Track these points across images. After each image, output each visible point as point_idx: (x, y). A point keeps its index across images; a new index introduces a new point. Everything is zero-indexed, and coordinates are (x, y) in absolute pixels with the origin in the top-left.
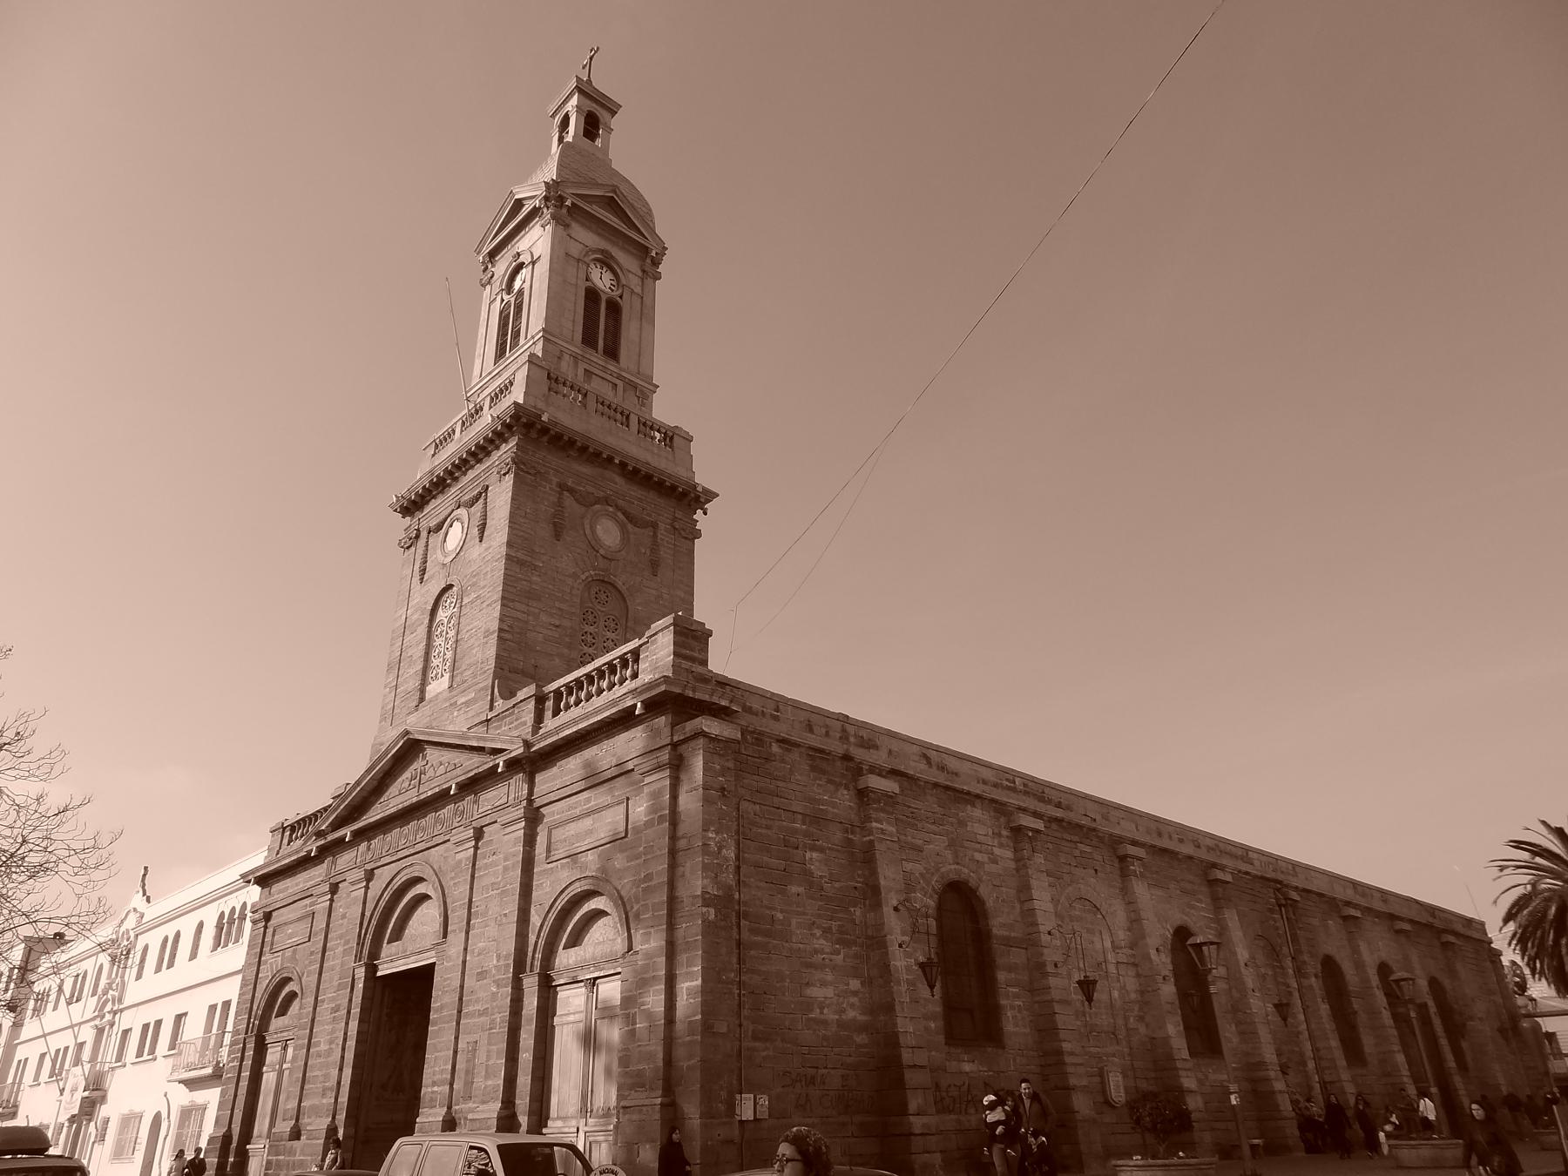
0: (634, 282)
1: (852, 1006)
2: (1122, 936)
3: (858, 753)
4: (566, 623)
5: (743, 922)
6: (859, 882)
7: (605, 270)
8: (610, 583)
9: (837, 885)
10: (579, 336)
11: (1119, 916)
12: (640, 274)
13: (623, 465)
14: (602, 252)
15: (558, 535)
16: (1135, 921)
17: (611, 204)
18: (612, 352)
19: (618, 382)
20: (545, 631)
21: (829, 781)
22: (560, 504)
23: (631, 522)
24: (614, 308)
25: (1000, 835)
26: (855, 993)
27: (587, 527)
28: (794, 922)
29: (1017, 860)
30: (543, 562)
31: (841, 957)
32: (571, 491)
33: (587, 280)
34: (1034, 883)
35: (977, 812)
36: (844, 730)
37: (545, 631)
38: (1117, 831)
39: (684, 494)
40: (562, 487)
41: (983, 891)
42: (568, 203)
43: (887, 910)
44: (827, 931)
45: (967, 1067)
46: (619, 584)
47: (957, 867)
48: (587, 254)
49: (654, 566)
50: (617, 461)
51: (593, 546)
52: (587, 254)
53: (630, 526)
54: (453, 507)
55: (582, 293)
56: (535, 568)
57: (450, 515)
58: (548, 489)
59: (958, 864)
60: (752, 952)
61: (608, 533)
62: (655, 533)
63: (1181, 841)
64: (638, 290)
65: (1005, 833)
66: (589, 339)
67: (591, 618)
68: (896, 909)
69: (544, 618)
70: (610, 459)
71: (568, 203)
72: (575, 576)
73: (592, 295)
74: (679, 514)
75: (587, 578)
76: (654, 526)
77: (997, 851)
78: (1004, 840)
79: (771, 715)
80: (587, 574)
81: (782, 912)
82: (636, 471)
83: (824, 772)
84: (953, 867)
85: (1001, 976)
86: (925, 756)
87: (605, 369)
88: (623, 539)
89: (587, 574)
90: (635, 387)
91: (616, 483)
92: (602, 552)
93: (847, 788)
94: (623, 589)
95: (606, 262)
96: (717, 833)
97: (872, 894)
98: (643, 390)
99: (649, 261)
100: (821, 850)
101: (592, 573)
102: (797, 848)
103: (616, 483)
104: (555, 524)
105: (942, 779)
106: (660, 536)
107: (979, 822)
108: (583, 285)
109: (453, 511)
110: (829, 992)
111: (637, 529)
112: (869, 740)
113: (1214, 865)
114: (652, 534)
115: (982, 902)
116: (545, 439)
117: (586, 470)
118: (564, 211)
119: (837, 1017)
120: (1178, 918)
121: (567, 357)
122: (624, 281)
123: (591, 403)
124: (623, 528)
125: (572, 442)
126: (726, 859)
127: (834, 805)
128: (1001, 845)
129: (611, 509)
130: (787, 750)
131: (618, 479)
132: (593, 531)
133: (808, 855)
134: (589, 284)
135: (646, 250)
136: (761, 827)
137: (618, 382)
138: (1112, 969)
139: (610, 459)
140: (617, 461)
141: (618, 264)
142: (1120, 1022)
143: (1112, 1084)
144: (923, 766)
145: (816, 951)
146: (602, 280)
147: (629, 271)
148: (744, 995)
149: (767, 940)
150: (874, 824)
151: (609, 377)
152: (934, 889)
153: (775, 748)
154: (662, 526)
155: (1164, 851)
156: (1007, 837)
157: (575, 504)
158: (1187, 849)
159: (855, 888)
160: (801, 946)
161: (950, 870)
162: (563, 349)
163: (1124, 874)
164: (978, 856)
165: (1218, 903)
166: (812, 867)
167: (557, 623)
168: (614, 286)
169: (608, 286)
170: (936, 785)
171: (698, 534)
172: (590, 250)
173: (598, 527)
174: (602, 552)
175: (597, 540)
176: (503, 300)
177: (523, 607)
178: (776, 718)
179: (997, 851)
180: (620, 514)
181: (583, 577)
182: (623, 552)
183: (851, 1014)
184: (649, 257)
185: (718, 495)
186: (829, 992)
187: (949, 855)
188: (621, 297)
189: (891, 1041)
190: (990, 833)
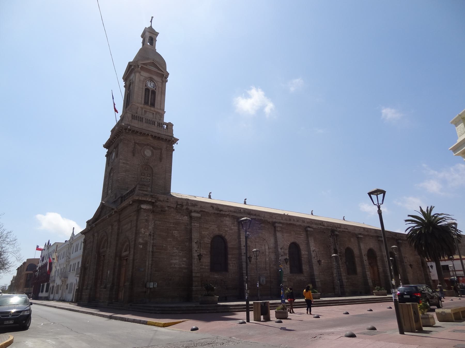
0: (160, 84)
1: (183, 264)
2: (272, 245)
3: (190, 208)
5: (154, 247)
6: (188, 237)
7: (151, 82)
9: (182, 238)
10: (143, 102)
11: (272, 240)
12: (161, 81)
13: (152, 136)
14: (150, 78)
15: (134, 155)
16: (276, 242)
17: (153, 64)
18: (153, 105)
19: (154, 112)
24: (154, 93)
26: (185, 261)
27: (142, 152)
28: (168, 247)
30: (130, 162)
31: (181, 253)
32: (138, 144)
33: (146, 86)
35: (228, 219)
36: (187, 202)
38: (274, 220)
39: (170, 141)
41: (226, 237)
42: (140, 67)
44: (177, 249)
45: (216, 277)
47: (219, 232)
48: (146, 79)
49: (161, 159)
50: (150, 135)
52: (146, 79)
53: (154, 151)
55: (144, 90)
56: (128, 164)
58: (131, 144)
59: (219, 231)
60: (156, 254)
61: (148, 153)
62: (161, 151)
63: (298, 221)
64: (161, 86)
66: (146, 103)
67: (143, 174)
70: (148, 135)
71: (140, 67)
73: (147, 90)
74: (168, 146)
75: (142, 165)
76: (161, 149)
77: (232, 227)
79: (166, 201)
80: (142, 164)
81: (165, 245)
82: (155, 137)
83: (180, 213)
84: (218, 232)
85: (229, 256)
86: (212, 206)
87: (150, 110)
88: (152, 154)
90: (159, 113)
91: (150, 140)
92: (146, 158)
93: (187, 216)
95: (151, 80)
96: (144, 229)
97: (190, 240)
98: (161, 114)
99: (164, 78)
100: (178, 230)
101: (143, 163)
102: (171, 230)
103: (150, 140)
104: (133, 153)
105: (216, 212)
106: (162, 152)
107: (228, 221)
108: (144, 88)
110: (177, 261)
112: (195, 204)
113: (309, 227)
114: (160, 152)
116: (130, 132)
118: (139, 68)
119: (179, 266)
120: (292, 240)
121: (139, 108)
122: (156, 84)
123: (144, 120)
125: (137, 132)
126: (146, 235)
127: (183, 220)
128: (234, 226)
129: (149, 147)
130: (170, 208)
132: (144, 153)
133: (174, 232)
134: (146, 87)
135: (163, 75)
136: (161, 226)
137: (154, 112)
138: (267, 253)
139: (148, 135)
140: (150, 135)
141: (155, 80)
143: (261, 280)
144: (211, 209)
145: (174, 253)
146: (150, 85)
147: (158, 81)
148: (153, 262)
149: (161, 251)
150: (193, 224)
151: (151, 112)
152: (211, 237)
153: (166, 208)
154: (163, 149)
155: (291, 224)
156: (236, 224)
158: (298, 223)
159: (187, 238)
160: (170, 252)
161: (217, 232)
162: (139, 106)
163: (275, 231)
164: (226, 229)
165: (308, 235)
166: (175, 234)
167: (134, 177)
168: (154, 86)
169: (152, 86)
170: (214, 213)
171: (174, 150)
172: (147, 78)
173: (145, 152)
174: (146, 158)
176: (127, 92)
177: (124, 174)
178: (168, 202)
180: (151, 148)
181: (141, 165)
182: (152, 157)
183: (183, 266)
184: (164, 76)
185: (179, 140)
186: (177, 261)
187: (217, 229)
188: (156, 89)
189: (191, 272)
190: (231, 223)
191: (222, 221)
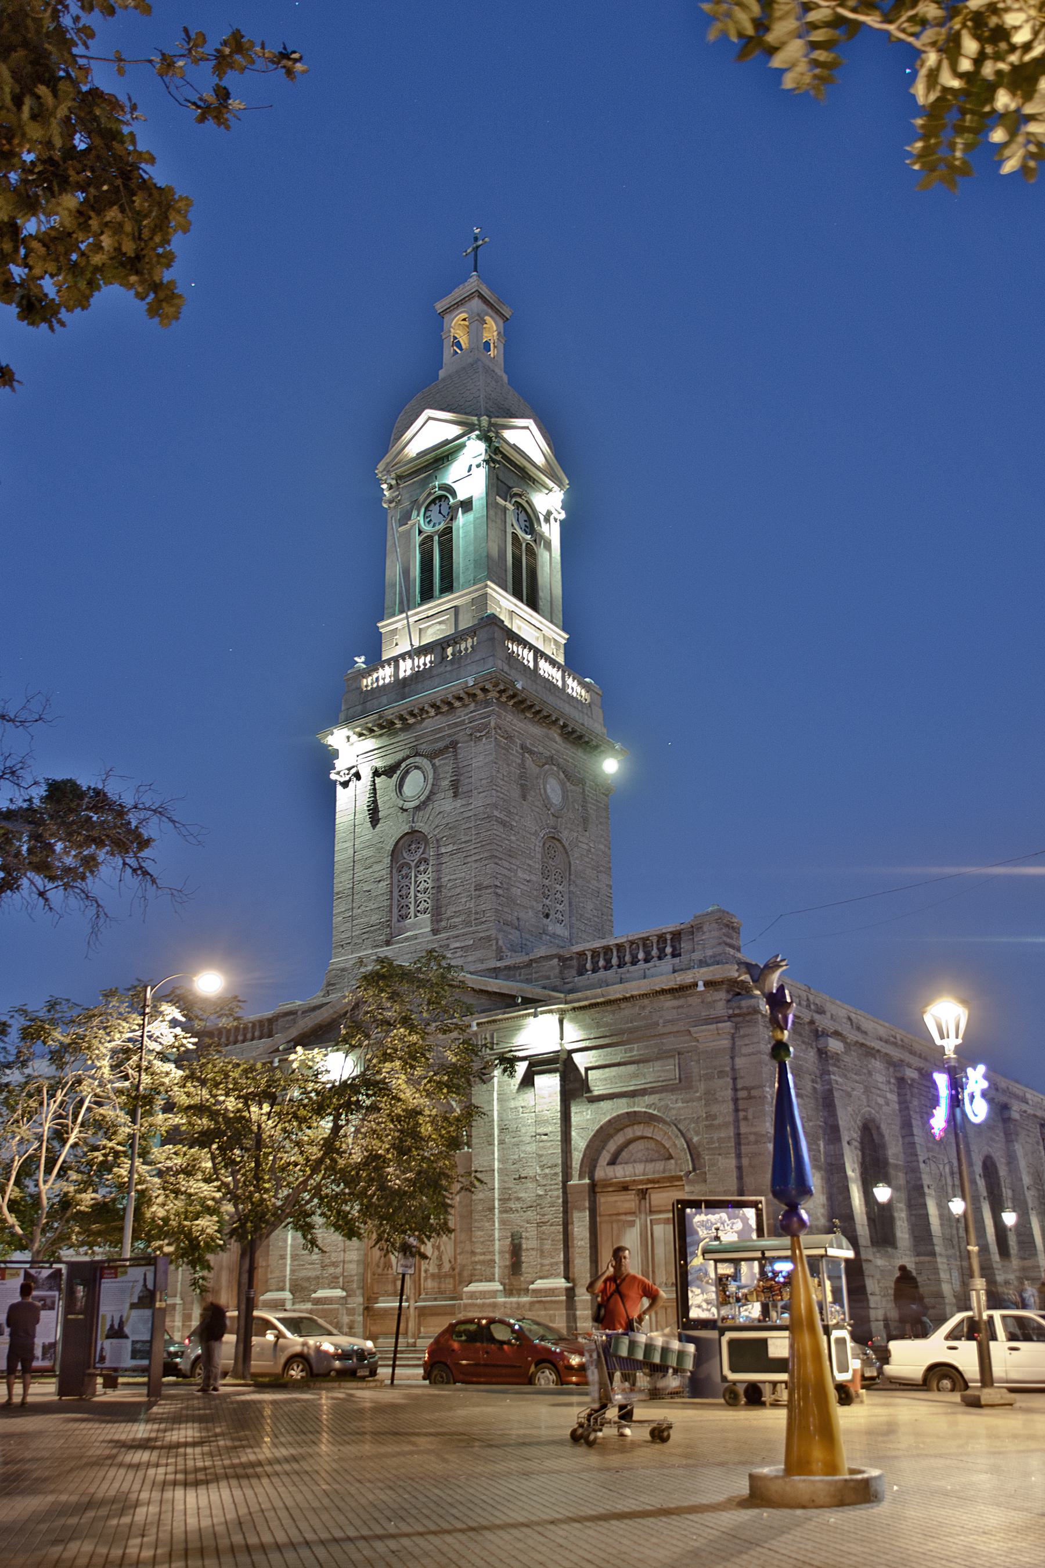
4: (534, 878)
8: (558, 840)
15: (524, 797)
20: (522, 887)
21: (803, 1042)
22: (522, 765)
23: (569, 780)
25: (889, 1082)
29: (900, 1103)
32: (531, 752)
34: (914, 1122)
37: (522, 887)
40: (523, 747)
43: (845, 1144)
46: (564, 841)
51: (547, 804)
54: (407, 752)
57: (404, 760)
65: (893, 1081)
68: (849, 1143)
69: (520, 874)
72: (536, 834)
77: (889, 1095)
78: (892, 1086)
80: (544, 832)
89: (544, 832)
94: (567, 844)
104: (522, 785)
109: (408, 757)
111: (573, 787)
115: (881, 1136)
117: (536, 730)
124: (563, 785)
128: (891, 1091)
131: (558, 738)
142: (955, 1232)
157: (533, 766)
170: (857, 1042)
175: (548, 797)
179: (889, 1095)
191: (870, 1073)
